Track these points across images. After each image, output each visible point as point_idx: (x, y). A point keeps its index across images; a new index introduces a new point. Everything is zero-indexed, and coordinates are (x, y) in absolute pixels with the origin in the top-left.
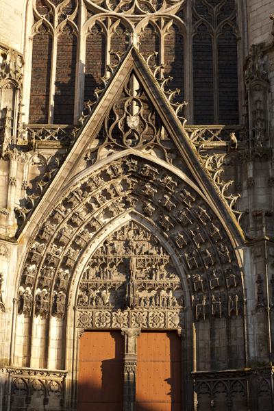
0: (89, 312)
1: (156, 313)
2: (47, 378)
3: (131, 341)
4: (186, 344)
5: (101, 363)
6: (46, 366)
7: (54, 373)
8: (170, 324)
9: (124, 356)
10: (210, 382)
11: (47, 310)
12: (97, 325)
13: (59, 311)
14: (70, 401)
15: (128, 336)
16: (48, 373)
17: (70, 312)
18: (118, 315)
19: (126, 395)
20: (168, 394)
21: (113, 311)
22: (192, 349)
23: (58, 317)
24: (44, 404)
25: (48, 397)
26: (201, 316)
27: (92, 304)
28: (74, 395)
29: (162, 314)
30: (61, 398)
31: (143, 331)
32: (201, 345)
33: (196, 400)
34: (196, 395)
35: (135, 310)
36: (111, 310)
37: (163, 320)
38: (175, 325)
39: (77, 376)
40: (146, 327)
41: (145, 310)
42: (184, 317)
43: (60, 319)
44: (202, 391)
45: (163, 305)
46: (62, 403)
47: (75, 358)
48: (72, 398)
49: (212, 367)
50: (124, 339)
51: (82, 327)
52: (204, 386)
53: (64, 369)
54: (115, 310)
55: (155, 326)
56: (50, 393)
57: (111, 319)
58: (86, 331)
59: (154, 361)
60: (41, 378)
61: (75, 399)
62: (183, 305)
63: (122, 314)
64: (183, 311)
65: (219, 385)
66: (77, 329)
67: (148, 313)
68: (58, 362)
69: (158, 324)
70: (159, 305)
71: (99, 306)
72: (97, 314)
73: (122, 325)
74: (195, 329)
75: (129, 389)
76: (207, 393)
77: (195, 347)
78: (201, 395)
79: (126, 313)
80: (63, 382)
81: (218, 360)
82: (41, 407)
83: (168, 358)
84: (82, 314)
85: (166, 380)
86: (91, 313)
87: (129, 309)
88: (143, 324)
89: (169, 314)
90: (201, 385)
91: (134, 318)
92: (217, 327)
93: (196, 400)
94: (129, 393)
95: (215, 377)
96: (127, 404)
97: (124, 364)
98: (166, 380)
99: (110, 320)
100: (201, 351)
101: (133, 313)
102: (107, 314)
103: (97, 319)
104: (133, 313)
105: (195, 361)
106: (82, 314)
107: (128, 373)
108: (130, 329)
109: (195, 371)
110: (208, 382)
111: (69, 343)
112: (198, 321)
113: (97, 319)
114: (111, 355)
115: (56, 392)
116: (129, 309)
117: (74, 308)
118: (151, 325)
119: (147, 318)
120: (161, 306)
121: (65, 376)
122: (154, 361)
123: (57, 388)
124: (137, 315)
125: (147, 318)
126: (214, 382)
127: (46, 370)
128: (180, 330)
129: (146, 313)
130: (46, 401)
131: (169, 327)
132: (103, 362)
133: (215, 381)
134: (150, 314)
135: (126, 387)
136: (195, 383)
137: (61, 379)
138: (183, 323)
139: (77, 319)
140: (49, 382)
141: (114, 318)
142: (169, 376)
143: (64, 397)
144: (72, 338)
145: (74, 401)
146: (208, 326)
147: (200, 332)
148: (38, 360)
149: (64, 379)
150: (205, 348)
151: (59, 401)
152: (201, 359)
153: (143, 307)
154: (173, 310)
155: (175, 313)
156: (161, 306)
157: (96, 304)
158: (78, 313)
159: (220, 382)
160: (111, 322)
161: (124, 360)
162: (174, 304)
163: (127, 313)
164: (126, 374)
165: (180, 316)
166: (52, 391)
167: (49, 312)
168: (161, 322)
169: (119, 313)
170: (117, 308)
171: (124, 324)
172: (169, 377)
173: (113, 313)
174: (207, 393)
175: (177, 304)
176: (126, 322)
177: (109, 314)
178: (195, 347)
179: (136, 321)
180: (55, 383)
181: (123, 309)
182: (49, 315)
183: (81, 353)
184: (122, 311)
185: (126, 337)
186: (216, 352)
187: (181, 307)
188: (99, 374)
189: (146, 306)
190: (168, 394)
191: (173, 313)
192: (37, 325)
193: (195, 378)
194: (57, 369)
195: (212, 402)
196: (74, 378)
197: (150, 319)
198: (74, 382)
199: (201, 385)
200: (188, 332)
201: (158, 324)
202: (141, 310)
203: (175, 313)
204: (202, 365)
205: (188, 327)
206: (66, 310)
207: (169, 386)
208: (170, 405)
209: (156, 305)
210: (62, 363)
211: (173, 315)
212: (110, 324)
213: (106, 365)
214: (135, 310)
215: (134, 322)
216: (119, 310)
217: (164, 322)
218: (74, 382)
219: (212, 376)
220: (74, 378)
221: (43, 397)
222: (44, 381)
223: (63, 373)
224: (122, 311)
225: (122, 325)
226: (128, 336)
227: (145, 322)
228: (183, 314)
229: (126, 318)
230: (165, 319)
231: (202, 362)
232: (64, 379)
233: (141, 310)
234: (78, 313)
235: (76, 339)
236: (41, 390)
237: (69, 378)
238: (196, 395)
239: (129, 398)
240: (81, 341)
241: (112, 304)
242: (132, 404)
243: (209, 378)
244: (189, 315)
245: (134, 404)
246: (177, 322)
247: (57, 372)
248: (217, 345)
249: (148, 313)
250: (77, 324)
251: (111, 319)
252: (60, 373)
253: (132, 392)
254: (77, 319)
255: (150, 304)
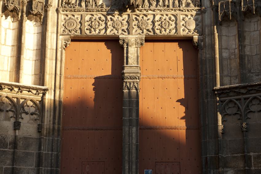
0: (77, 16)
1: (165, 17)
2: (19, 95)
3: (132, 52)
4: (204, 54)
5: (93, 81)
6: (18, 79)
7: (29, 89)
8: (184, 30)
9: (123, 68)
10: (240, 99)
11: (19, 7)
12: (88, 32)
13: (35, 12)
14: (51, 128)
15: (127, 45)
16: (21, 88)
17: (52, 14)
18: (115, 19)
19: (126, 118)
20: (182, 118)
21: (108, 14)
22: (214, 58)
23: (36, 21)
24: (15, 130)
25: (20, 120)
26: (225, 16)
27: (80, 5)
28: (57, 121)
29: (173, 18)
30: (39, 122)
31: (148, 40)
32: (225, 55)
33: (220, 123)
34: (220, 117)
35: (138, 12)
36: (106, 13)
37: (174, 25)
38: (189, 31)
39: (62, 95)
40: (152, 34)
41: (150, 12)
42: (202, 21)
43: (39, 24)
44: (228, 112)
45: (173, 7)
46: (40, 129)
47: (58, 72)
48: (54, 123)
49: (242, 81)
50: (123, 48)
51: (68, 35)
52: (231, 105)
53: (43, 85)
54: (110, 13)
55: (163, 32)
56: (23, 115)
57: (106, 24)
58: (75, 40)
59: (162, 78)
60: (10, 95)
61: (59, 124)
62: (200, 6)
63: (120, 18)
64: (201, 13)
65: (254, 102)
66: (60, 37)
67: (154, 16)
68: (35, 77)
69: (168, 31)
70: (168, 6)
71: (90, 7)
72: (87, 18)
73: (120, 31)
74: (216, 35)
75: (130, 111)
76: (236, 114)
77: (217, 56)
78: (227, 118)
79: (125, 16)
80: (42, 101)
81: (250, 71)
82: (11, 132)
83: (181, 73)
84: (67, 18)
85: (178, 101)
86: (79, 17)
87: (129, 11)
88: (148, 30)
89: (182, 17)
90: (227, 104)
91: (135, 22)
92: (247, 30)
93: (220, 123)
94: (130, 115)
95: (248, 92)
96: (127, 129)
97: (123, 79)
98: (178, 101)
99: (104, 26)
100: (225, 63)
101: (134, 17)
102: (100, 18)
103: (87, 24)
104: (134, 17)
105: (218, 73)
106: (67, 18)
107: (129, 89)
108: (130, 36)
109: (218, 86)
110: (237, 100)
111: (50, 53)
112: (221, 25)
113: (87, 24)
114: (107, 70)
115: (32, 114)
116: (129, 11)
117: (57, 11)
118: (158, 32)
119: (153, 22)
120: (171, 7)
121: (44, 94)
122: (162, 78)
123: (33, 110)
124: (140, 18)
125: (153, 22)
126: (245, 99)
127: (17, 84)
128: (196, 37)
129: (151, 17)
130: (17, 126)
131: (182, 33)
132: (96, 79)
133: (248, 98)
134: (157, 18)
135: (126, 108)
136: (218, 102)
137: (39, 98)
138: (200, 28)
139: (61, 23)
140: (21, 101)
141: (110, 23)
142: (182, 96)
143: (42, 121)
144: (55, 48)
145: (56, 127)
146: (233, 30)
147: (224, 38)
148: (9, 73)
149: (43, 98)
150: (230, 59)
151: (36, 126)
152: (225, 73)
153: (147, 8)
154: (187, 13)
155: (189, 16)
156: (171, 7)
157: (86, 6)
158: (62, 17)
159: (255, 98)
160: (106, 28)
161: (124, 73)
162: (188, 5)
163: (127, 17)
164: (126, 91)
165: (196, 20)
166: (27, 113)
167: (22, 12)
168: (171, 27)
169: (116, 16)
170: (113, 11)
171: (123, 30)
172: (182, 96)
173: (109, 17)
174: (236, 114)
175: (192, 5)
176: (125, 28)
177: (103, 18)
178: (217, 56)
179: (138, 27)
180: (30, 103)
181: (122, 11)
182: (22, 16)
183: (66, 69)
184: (120, 15)
185: (125, 46)
186: (246, 62)
187: (197, 8)
188: (90, 91)
189: (153, 8)
190: (182, 118)
191: (187, 16)
192: (6, 29)
193: (219, 95)
194: (34, 85)
195: (244, 125)
196: (57, 98)
197: (156, 24)
198: (57, 103)
199: (227, 104)
200: (207, 40)
201: (168, 31)
202: (145, 12)
203: (189, 16)
204: (226, 80)
205: (207, 33)
206: (46, 11)
207: (183, 109)
208: (185, 131)
209: (164, 6)
210: (41, 77)
211: (187, 19)
212: (104, 31)
213: (99, 82)
214: (138, 12)
215: (136, 27)
216: (117, 13)
217: (176, 27)
218: (57, 103)
219: (243, 91)
220: (57, 98)
221: (13, 120)
222: (15, 100)
223: (41, 89)
224: (120, 15)
225: (120, 31)
226: (127, 45)
227: (150, 27)
228: (200, 17)
229: (125, 22)
230: (176, 23)
231: (227, 76)
232: (43, 98)
233: (145, 12)
234: (62, 17)
235: (59, 50)
236: (10, 111)
237: (49, 97)
238: (220, 117)
239: (130, 121)
240: (66, 53)
241: (107, 6)
242: (134, 129)
243: (239, 94)
244: (208, 18)
245: (137, 130)
246: (193, 26)
247: (33, 89)
248: (248, 53)
249: (154, 16)
250: (61, 30)
251: (106, 24)
252: (37, 90)
253: (134, 114)
254: (61, 23)
255: (156, 6)
